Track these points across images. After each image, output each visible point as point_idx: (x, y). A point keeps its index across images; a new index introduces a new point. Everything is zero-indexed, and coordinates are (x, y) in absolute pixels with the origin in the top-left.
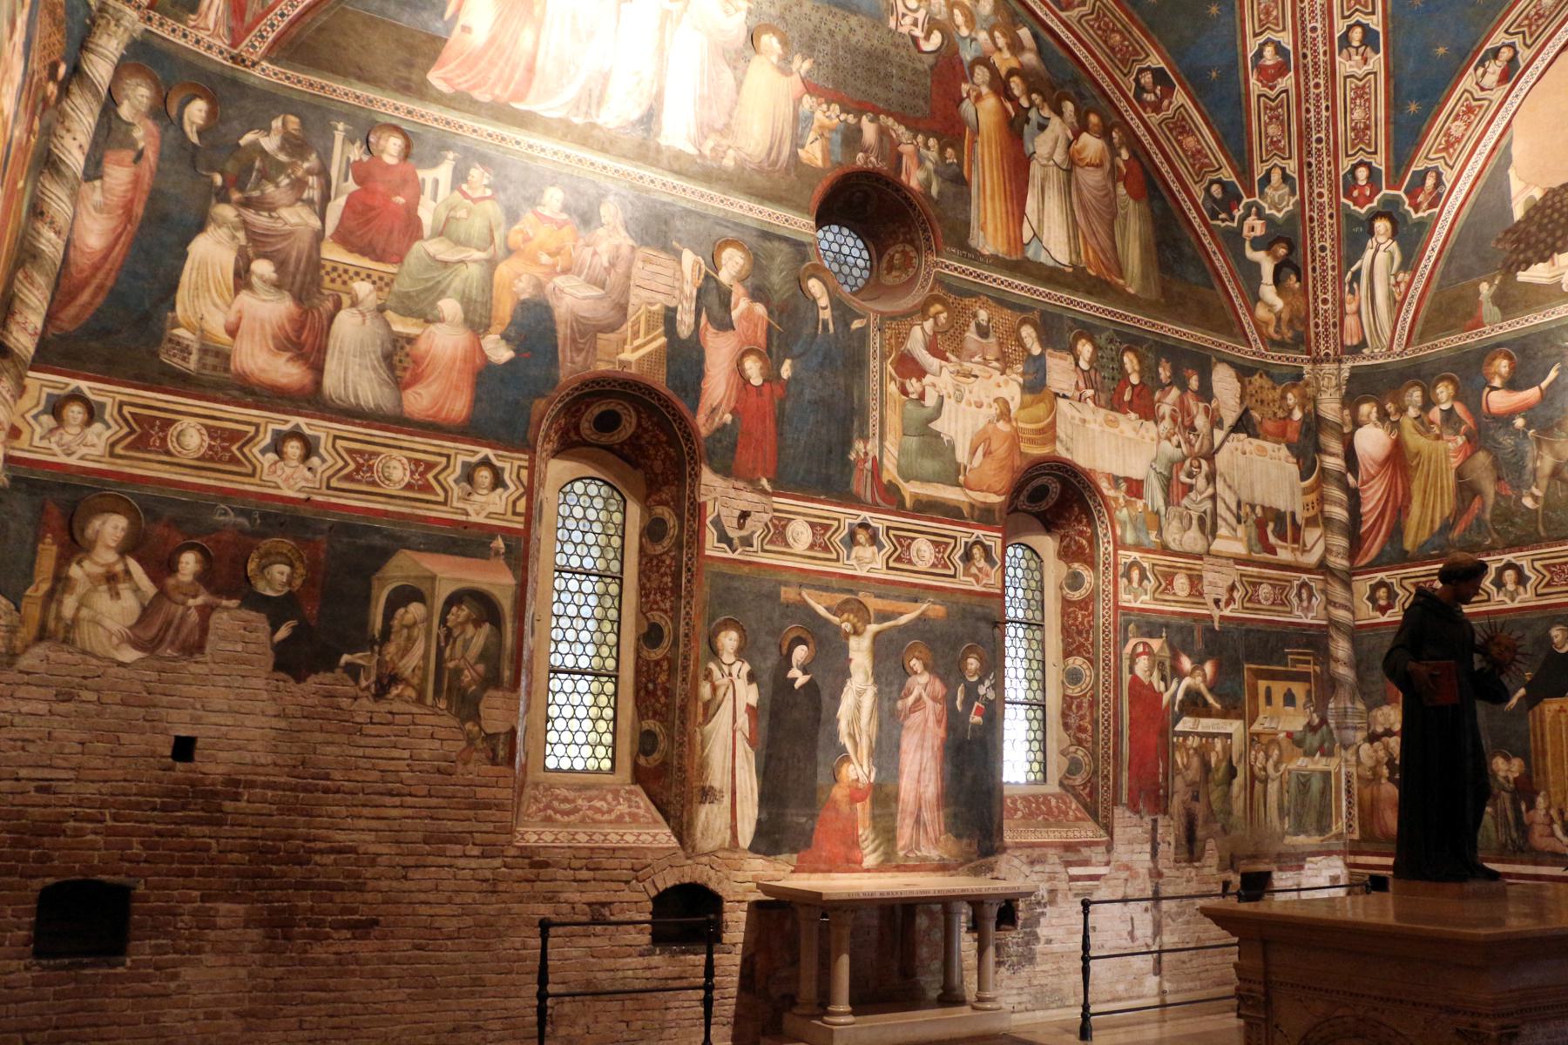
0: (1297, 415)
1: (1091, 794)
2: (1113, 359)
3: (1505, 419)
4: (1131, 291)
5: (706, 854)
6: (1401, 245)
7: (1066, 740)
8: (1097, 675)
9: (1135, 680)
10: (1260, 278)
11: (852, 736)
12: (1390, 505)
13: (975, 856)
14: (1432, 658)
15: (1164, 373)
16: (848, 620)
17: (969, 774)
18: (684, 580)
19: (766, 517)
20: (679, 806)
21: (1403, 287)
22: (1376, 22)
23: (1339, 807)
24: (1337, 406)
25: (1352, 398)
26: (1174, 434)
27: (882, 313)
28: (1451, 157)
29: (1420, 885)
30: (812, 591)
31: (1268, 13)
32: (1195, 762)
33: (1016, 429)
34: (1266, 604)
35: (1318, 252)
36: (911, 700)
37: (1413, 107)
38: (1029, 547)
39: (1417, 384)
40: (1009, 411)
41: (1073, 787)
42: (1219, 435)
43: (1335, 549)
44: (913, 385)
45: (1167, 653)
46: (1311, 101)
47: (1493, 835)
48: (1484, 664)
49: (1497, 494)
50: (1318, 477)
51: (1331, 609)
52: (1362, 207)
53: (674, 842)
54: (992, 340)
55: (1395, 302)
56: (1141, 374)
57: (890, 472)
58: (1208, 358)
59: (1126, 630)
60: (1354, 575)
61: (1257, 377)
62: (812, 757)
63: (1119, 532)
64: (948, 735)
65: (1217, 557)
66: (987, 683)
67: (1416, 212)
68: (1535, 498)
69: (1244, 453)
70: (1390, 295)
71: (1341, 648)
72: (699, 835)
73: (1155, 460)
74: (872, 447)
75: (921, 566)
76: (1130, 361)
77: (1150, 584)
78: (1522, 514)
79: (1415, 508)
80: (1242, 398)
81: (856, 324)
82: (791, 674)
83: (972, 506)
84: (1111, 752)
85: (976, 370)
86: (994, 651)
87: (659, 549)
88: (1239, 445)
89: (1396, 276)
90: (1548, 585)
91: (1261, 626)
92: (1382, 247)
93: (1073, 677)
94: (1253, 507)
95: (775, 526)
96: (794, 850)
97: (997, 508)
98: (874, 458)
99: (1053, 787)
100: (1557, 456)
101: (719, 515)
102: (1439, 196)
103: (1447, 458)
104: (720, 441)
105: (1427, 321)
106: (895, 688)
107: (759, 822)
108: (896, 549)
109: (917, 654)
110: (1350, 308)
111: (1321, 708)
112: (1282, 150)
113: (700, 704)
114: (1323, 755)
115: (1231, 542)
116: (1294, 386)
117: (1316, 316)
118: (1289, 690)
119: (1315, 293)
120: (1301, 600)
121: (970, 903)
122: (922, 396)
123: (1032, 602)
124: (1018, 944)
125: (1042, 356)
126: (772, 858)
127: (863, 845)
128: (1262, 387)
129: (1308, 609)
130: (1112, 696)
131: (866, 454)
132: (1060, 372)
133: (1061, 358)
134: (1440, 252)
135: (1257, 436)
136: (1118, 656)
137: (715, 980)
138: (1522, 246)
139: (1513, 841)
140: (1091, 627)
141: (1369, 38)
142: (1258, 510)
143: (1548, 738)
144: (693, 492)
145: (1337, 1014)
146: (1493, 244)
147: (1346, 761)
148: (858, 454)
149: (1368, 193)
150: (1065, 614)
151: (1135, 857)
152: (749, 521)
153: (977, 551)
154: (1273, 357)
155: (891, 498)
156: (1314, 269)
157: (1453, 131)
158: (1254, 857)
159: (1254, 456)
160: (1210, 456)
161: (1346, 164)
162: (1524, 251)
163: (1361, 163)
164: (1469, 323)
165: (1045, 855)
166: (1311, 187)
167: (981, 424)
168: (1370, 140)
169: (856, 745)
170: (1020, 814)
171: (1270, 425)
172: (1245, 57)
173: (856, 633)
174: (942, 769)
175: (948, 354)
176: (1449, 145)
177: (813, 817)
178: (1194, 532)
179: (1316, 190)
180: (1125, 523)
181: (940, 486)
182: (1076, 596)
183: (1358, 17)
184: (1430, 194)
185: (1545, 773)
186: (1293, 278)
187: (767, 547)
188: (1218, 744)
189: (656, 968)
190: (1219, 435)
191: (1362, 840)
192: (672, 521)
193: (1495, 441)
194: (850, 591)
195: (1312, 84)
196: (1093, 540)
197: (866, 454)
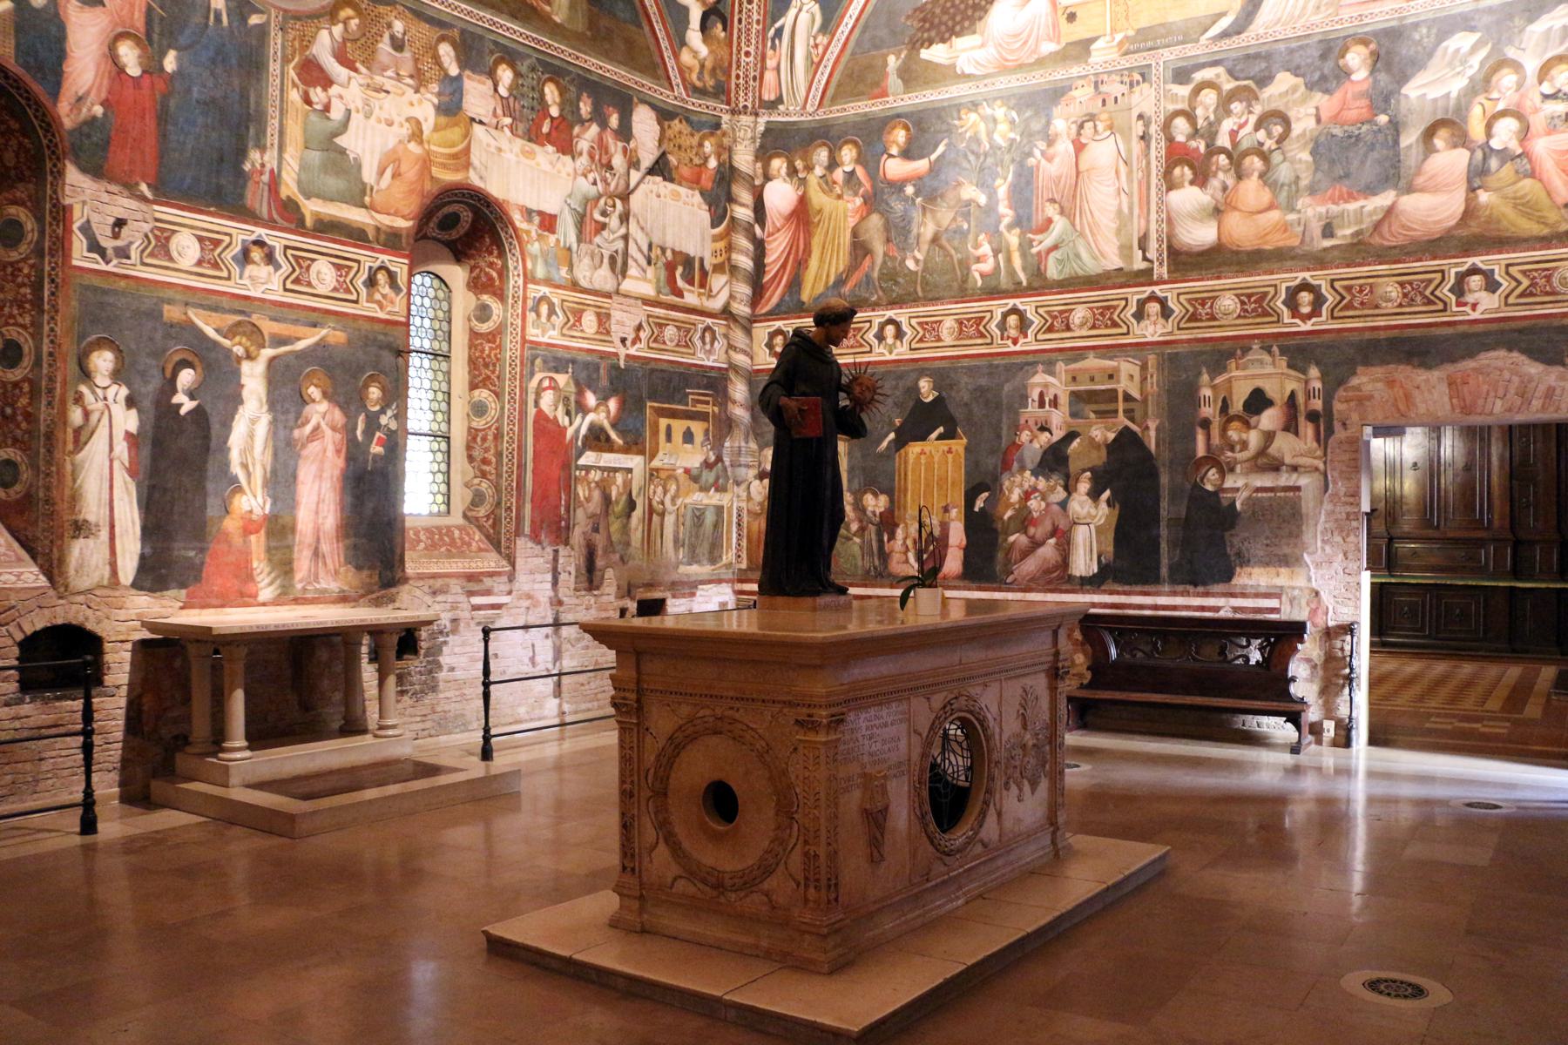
0: (713, 163)
1: (494, 526)
2: (533, 89)
3: (897, 186)
4: (557, 19)
5: (80, 593)
6: (822, 8)
8: (502, 408)
9: (540, 414)
10: (688, 22)
11: (245, 466)
12: (792, 257)
13: (376, 588)
14: (804, 394)
15: (585, 108)
16: (240, 344)
17: (369, 506)
18: (46, 293)
19: (146, 227)
21: (821, 49)
23: (729, 539)
24: (750, 158)
25: (764, 154)
26: (591, 171)
27: (285, 11)
29: (780, 600)
30: (201, 311)
32: (596, 494)
33: (428, 153)
34: (670, 345)
36: (308, 429)
38: (437, 276)
39: (824, 144)
40: (421, 132)
41: (477, 519)
43: (738, 296)
44: (317, 95)
45: (573, 389)
47: (860, 563)
48: (848, 403)
49: (885, 254)
50: (728, 225)
51: (731, 353)
53: (43, 581)
54: (407, 54)
55: (812, 62)
56: (562, 110)
58: (630, 99)
59: (533, 363)
60: (755, 321)
61: (677, 121)
63: (529, 265)
64: (348, 465)
65: (626, 296)
66: (389, 413)
68: (917, 261)
69: (659, 196)
70: (809, 56)
71: (739, 391)
72: (72, 572)
73: (570, 196)
74: (270, 158)
75: (321, 290)
76: (551, 92)
77: (559, 319)
78: (905, 275)
79: (814, 263)
80: (660, 141)
81: (254, 20)
82: (176, 400)
83: (378, 229)
84: (514, 484)
85: (389, 84)
86: (397, 380)
88: (655, 188)
89: (815, 38)
90: (921, 340)
91: (665, 366)
92: (805, 8)
93: (479, 409)
94: (663, 250)
95: (157, 237)
96: (182, 585)
98: (272, 171)
99: (456, 519)
100: (938, 224)
101: (88, 221)
103: (846, 217)
105: (839, 85)
106: (292, 416)
107: (142, 557)
108: (294, 270)
110: (770, 63)
111: (717, 446)
113: (70, 431)
114: (717, 490)
115: (641, 282)
116: (712, 134)
117: (738, 67)
118: (689, 428)
119: (739, 44)
120: (704, 343)
121: (370, 633)
122: (327, 108)
123: (439, 333)
124: (420, 673)
125: (459, 78)
126: (158, 594)
127: (258, 579)
128: (680, 133)
129: (710, 352)
130: (516, 429)
132: (478, 96)
133: (479, 82)
134: (857, 20)
135: (672, 180)
136: (524, 390)
138: (927, 25)
139: (875, 568)
140: (498, 359)
142: (669, 254)
143: (910, 477)
145: (700, 715)
147: (738, 496)
148: (253, 165)
150: (471, 346)
151: (536, 586)
152: (125, 231)
153: (382, 277)
154: (695, 104)
155: (290, 217)
156: (740, 21)
158: (650, 585)
159: (668, 200)
160: (625, 197)
162: (929, 30)
164: (876, 91)
165: (448, 586)
167: (392, 143)
169: (249, 475)
170: (422, 545)
171: (685, 171)
175: (358, 65)
177: (202, 550)
178: (605, 270)
180: (536, 256)
181: (344, 206)
182: (484, 328)
185: (905, 508)
186: (720, 26)
188: (619, 478)
190: (635, 176)
191: (749, 569)
193: (887, 204)
194: (242, 312)
197: (263, 165)
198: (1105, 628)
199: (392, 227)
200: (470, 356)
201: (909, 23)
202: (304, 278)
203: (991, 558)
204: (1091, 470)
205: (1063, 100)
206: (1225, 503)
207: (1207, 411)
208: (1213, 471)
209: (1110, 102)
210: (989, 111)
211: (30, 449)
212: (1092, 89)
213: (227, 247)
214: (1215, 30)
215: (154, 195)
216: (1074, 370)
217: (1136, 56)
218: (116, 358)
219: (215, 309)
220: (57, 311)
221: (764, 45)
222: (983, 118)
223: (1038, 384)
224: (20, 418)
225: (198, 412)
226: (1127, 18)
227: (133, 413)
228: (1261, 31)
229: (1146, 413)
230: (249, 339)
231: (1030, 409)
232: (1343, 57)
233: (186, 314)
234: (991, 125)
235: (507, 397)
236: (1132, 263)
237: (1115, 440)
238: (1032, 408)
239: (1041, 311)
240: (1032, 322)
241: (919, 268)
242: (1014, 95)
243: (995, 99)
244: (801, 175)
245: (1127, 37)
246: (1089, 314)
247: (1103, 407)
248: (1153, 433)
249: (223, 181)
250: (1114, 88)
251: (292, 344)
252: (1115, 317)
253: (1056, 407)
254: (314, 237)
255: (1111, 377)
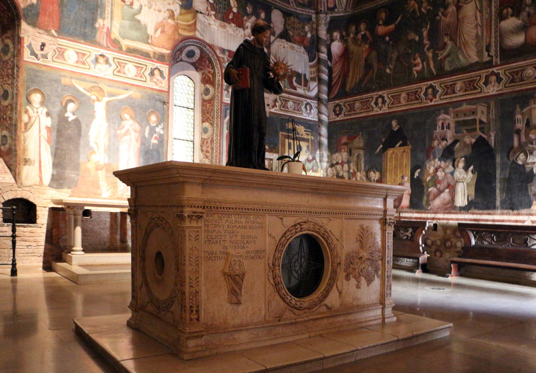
0: (309, 35)
5: (27, 186)
7: (202, 156)
11: (97, 143)
12: (342, 74)
16: (94, 95)
19: (55, 47)
20: (15, 166)
30: (77, 81)
33: (177, 24)
42: (272, 38)
49: (378, 68)
53: (13, 181)
57: (115, 34)
61: (292, 18)
62: (77, 150)
64: (141, 146)
68: (390, 69)
69: (284, 47)
74: (107, 23)
75: (129, 76)
82: (67, 115)
83: (155, 53)
84: (218, 161)
86: (163, 114)
87: (7, 58)
88: (282, 44)
90: (392, 104)
95: (59, 51)
96: (69, 188)
97: (166, 55)
98: (108, 28)
103: (362, 53)
104: (31, 11)
106: (117, 125)
107: (53, 175)
109: (127, 112)
116: (308, 23)
120: (306, 109)
126: (59, 190)
128: (294, 22)
131: (104, 25)
135: (290, 41)
137: (16, 233)
144: (18, 32)
148: (99, 25)
152: (45, 48)
153: (156, 72)
155: (116, 45)
159: (289, 50)
167: (160, 19)
169: (98, 147)
171: (297, 38)
173: (98, 100)
174: (139, 160)
177: (78, 175)
181: (140, 43)
187: (55, 60)
189: (6, 232)
192: (11, 46)
196: (214, 75)
197: (104, 25)
198: (470, 230)
199: (160, 53)
200: (202, 110)
202: (122, 70)
203: (421, 199)
204: (465, 157)
206: (528, 170)
207: (520, 125)
208: (522, 154)
211: (10, 131)
213: (89, 56)
215: (58, 35)
216: (457, 111)
218: (42, 97)
219: (84, 80)
220: (18, 78)
223: (442, 119)
224: (8, 119)
225: (77, 122)
227: (49, 119)
229: (489, 129)
230: (98, 93)
231: (438, 130)
233: (71, 82)
235: (215, 125)
236: (483, 59)
237: (475, 143)
238: (438, 130)
239: (442, 85)
240: (438, 91)
241: (392, 72)
244: (345, 38)
246: (464, 86)
247: (469, 128)
248: (493, 138)
249: (87, 31)
251: (117, 96)
252: (475, 85)
253: (449, 129)
254: (126, 55)
255: (473, 113)
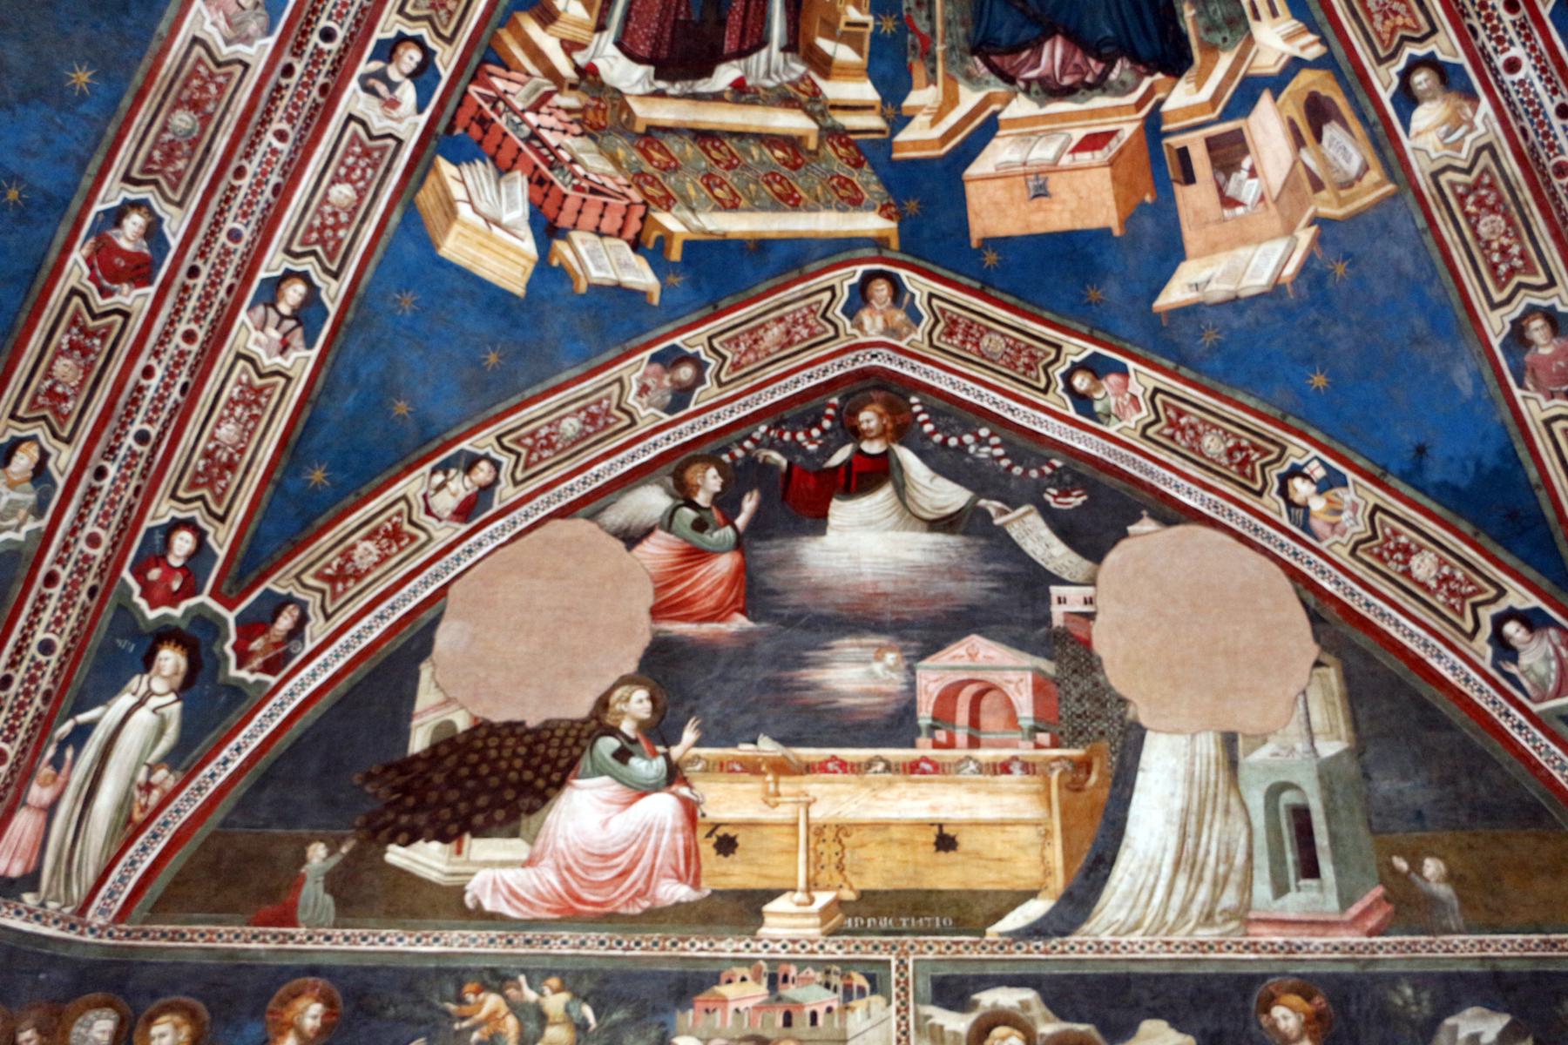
6: (184, 712)
21: (155, 795)
22: (333, 293)
28: (335, 596)
31: (169, 157)
35: (33, 650)
37: (318, 475)
39: (108, 1004)
46: (165, 358)
52: (153, 606)
55: (129, 820)
67: (240, 666)
89: (152, 769)
92: (154, 702)
102: (288, 656)
105: (179, 880)
110: (39, 793)
112: (63, 418)
141: (308, 314)
146: (357, 779)
149: (176, 585)
157: (357, 554)
161: (163, 510)
162: (413, 810)
163: (189, 524)
166: (81, 517)
168: (225, 490)
172: (88, 204)
176: (340, 576)
179: (90, 528)
183: (308, 265)
184: (277, 645)
195: (182, 328)
201: (369, 789)
205: (701, 1000)
209: (801, 1026)
210: (531, 995)
212: (761, 990)
214: (1016, 919)
217: (858, 939)
221: (38, 752)
222: (516, 1008)
226: (840, 868)
228: (1106, 938)
232: (1267, 1011)
234: (532, 1026)
242: (590, 972)
243: (549, 973)
245: (839, 903)
250: (812, 996)
